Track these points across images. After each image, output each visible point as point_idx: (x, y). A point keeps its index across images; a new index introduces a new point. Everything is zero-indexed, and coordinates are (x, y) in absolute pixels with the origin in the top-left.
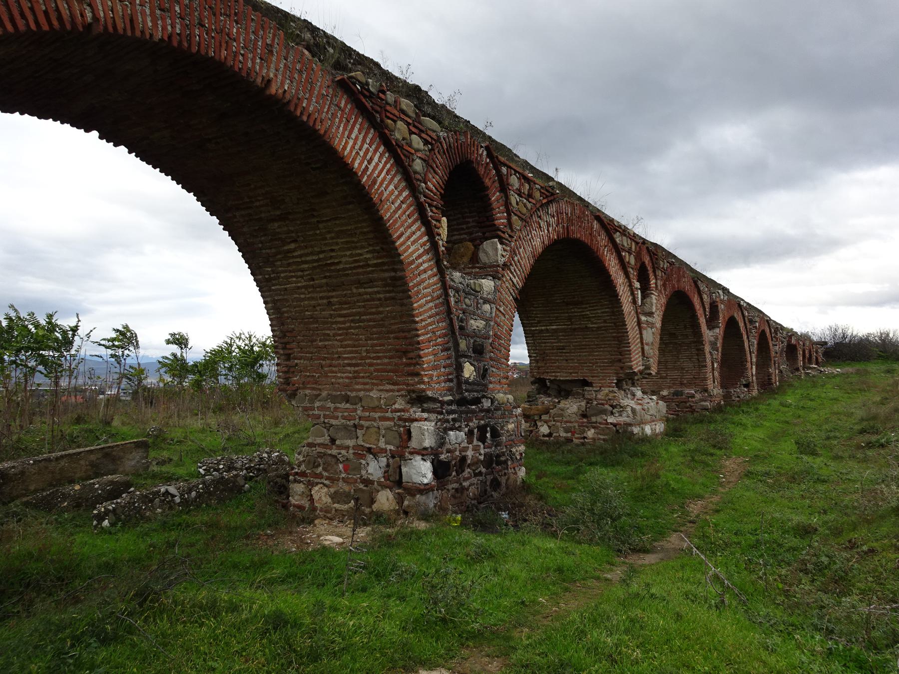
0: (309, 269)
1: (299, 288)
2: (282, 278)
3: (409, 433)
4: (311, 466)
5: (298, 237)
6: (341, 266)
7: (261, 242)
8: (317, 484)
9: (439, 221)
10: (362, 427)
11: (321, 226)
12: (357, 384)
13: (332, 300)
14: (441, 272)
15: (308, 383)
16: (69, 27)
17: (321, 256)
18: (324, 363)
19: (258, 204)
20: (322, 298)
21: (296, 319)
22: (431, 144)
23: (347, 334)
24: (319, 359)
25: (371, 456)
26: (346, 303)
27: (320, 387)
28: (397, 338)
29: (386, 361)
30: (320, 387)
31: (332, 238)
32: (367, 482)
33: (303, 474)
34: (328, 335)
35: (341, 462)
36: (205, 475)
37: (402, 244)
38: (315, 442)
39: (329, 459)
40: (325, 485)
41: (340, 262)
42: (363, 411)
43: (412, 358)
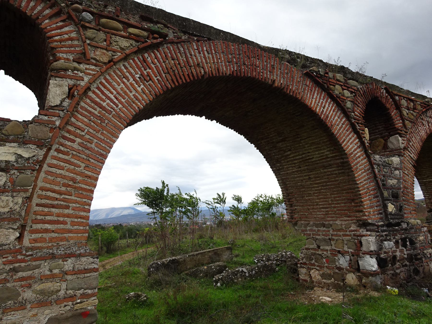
0: (298, 163)
1: (293, 172)
2: (285, 168)
3: (361, 243)
4: (309, 259)
5: (292, 148)
6: (314, 160)
7: (274, 153)
8: (313, 269)
9: (364, 130)
10: (333, 240)
11: (302, 141)
12: (328, 217)
13: (310, 176)
14: (368, 156)
15: (303, 218)
16: (196, 78)
17: (303, 156)
18: (309, 207)
19: (271, 136)
20: (305, 176)
21: (294, 187)
22: (354, 93)
23: (320, 193)
25: (341, 255)
26: (318, 177)
27: (309, 220)
28: (348, 193)
29: (343, 205)
30: (309, 220)
31: (308, 147)
32: (340, 269)
33: (305, 264)
34: (311, 194)
35: (324, 258)
36: (257, 263)
37: (345, 145)
38: (310, 248)
39: (318, 256)
40: (317, 270)
41: (313, 158)
42: (333, 231)
43: (357, 203)
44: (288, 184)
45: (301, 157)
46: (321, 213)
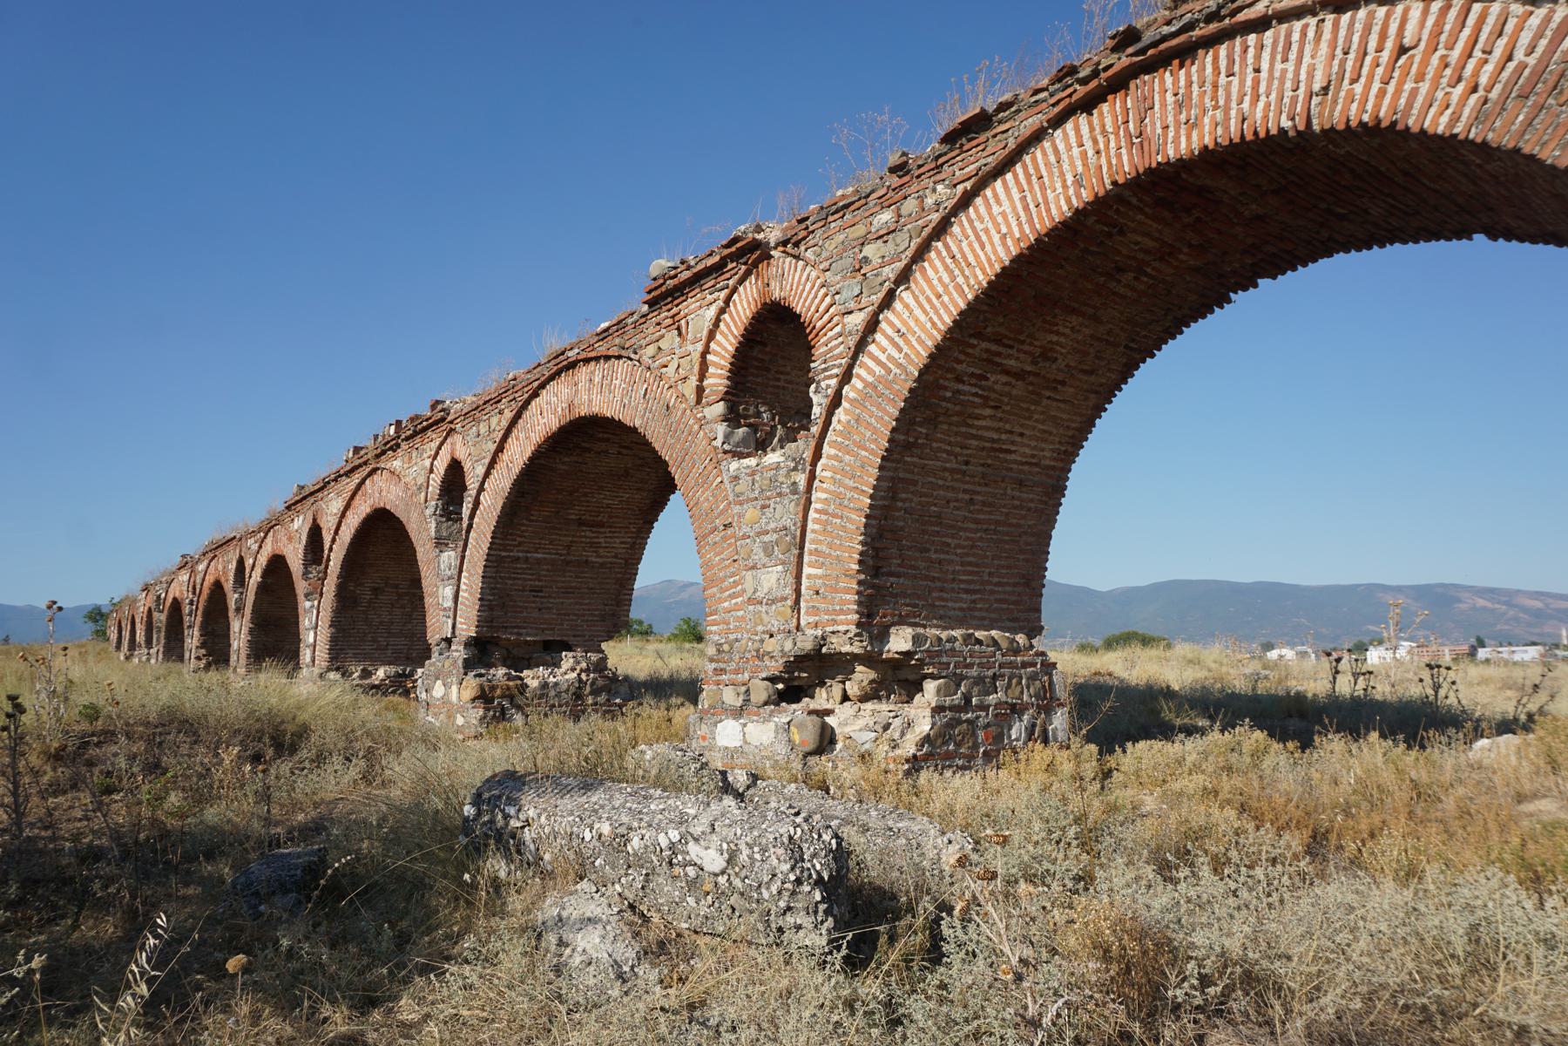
1: (945, 469)
6: (1013, 457)
13: (975, 497)
17: (1004, 437)
20: (965, 491)
24: (926, 578)
26: (990, 505)
29: (1008, 589)
34: (948, 545)
44: (904, 501)
45: (995, 436)
46: (958, 605)
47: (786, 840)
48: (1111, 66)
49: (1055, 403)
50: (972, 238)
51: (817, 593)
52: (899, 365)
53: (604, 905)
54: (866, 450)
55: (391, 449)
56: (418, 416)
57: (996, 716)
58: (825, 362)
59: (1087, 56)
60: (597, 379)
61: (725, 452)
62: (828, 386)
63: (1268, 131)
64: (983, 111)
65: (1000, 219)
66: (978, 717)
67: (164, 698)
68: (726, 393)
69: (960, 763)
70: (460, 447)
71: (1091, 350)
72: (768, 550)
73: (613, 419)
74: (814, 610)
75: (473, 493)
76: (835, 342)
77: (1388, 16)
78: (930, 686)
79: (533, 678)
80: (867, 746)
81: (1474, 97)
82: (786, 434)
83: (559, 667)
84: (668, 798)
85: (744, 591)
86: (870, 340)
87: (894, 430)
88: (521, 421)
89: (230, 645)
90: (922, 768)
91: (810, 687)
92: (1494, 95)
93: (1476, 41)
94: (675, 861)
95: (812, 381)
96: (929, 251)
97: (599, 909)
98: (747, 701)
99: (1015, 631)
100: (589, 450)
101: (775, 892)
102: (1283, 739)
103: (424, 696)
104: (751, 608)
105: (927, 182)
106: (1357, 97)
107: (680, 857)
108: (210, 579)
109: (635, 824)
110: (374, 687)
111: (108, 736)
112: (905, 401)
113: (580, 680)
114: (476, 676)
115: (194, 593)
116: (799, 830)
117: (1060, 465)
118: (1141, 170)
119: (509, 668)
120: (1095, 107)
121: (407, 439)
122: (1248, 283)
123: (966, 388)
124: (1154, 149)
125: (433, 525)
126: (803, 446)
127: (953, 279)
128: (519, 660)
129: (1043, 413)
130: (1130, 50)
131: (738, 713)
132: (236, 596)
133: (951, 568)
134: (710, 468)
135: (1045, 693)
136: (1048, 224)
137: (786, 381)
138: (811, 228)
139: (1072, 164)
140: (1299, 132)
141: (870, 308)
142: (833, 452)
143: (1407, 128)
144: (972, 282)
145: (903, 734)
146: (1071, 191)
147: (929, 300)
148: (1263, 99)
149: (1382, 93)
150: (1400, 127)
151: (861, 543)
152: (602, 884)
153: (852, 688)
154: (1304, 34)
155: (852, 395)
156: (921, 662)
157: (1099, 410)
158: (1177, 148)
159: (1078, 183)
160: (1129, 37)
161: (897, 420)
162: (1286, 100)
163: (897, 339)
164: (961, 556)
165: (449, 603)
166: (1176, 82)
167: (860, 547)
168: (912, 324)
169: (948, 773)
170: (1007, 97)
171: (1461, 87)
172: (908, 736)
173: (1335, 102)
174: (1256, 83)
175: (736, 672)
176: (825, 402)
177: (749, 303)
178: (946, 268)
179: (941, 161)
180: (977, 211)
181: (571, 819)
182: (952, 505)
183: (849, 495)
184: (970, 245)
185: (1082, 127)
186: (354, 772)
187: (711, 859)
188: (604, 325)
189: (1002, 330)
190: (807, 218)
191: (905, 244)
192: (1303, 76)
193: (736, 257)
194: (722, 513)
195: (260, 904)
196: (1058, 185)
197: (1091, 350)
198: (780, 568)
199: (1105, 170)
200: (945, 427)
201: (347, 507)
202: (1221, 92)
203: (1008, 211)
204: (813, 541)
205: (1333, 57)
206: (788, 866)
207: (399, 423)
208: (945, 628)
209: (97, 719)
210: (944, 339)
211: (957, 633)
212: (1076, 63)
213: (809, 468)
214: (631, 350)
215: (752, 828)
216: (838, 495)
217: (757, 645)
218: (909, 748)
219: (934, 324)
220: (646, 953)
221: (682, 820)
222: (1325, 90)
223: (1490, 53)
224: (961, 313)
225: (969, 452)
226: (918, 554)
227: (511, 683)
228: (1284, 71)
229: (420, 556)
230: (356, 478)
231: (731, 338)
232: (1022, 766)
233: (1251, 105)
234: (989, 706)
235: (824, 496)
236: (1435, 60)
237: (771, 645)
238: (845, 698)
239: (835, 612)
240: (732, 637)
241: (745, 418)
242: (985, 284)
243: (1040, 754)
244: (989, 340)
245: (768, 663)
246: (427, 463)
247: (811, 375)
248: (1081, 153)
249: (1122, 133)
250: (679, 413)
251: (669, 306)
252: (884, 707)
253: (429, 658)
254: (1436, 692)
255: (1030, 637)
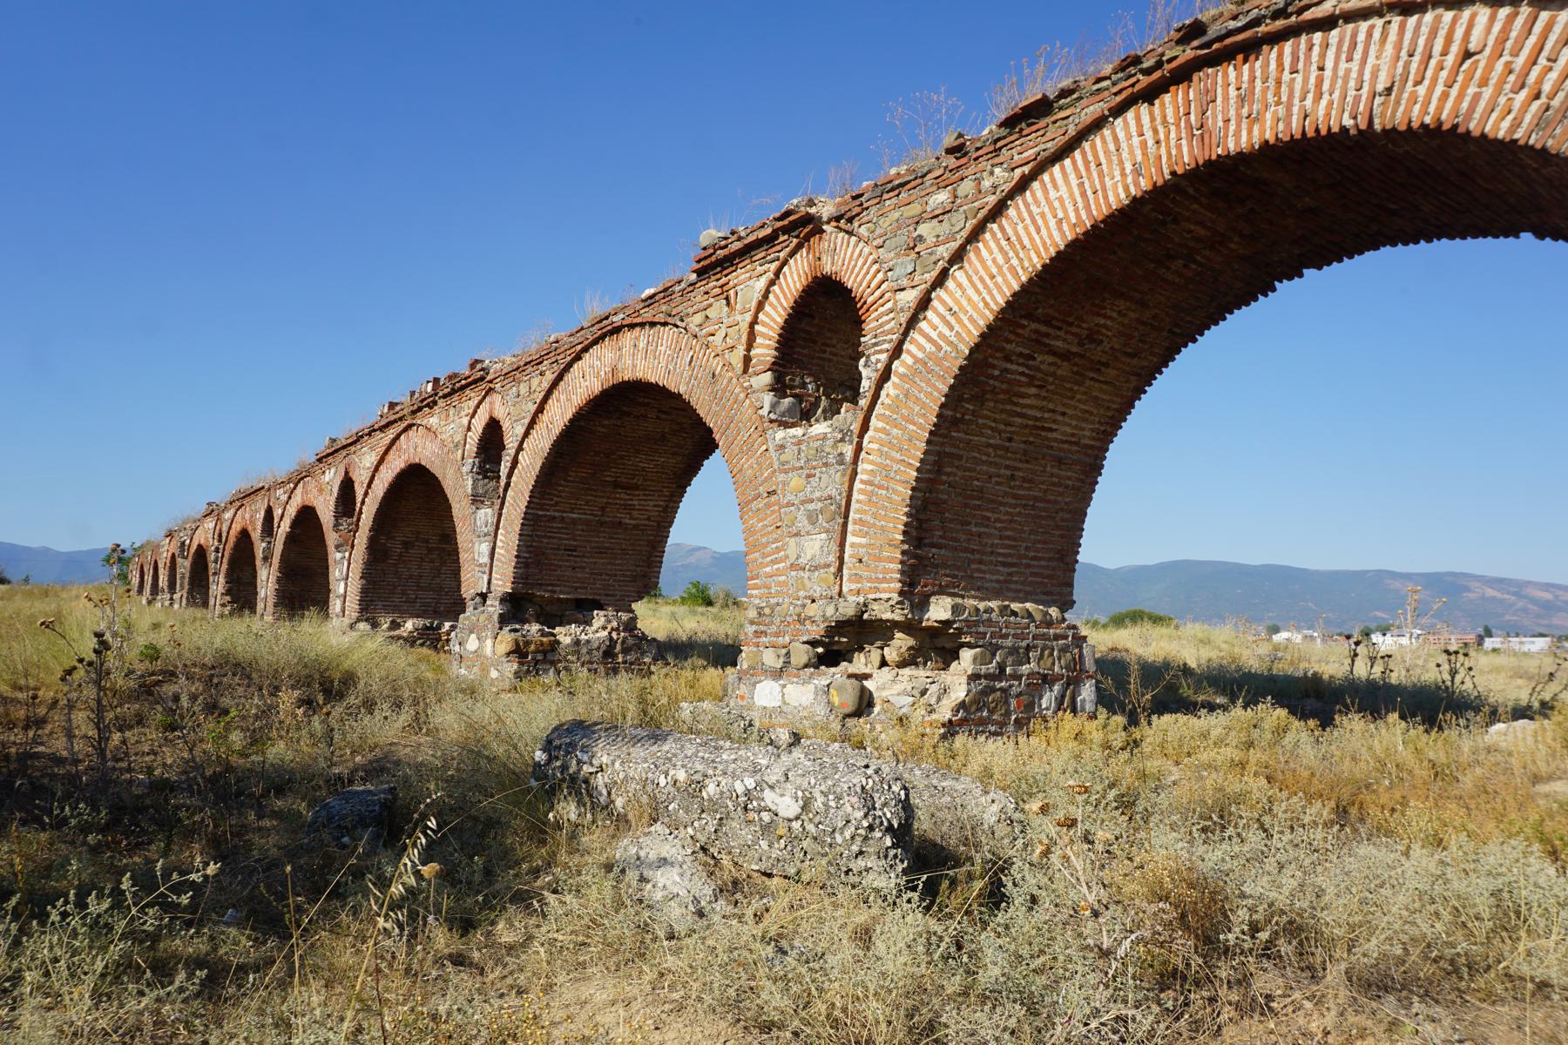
1: (989, 445)
6: (1054, 435)
13: (1016, 473)
17: (1046, 415)
20: (1007, 467)
24: (966, 550)
26: (1030, 481)
29: (1043, 563)
34: (988, 519)
44: (948, 474)
45: (1039, 415)
46: (995, 577)
47: (859, 790)
48: (1175, 58)
49: (1097, 385)
50: (1028, 221)
51: (860, 561)
52: (950, 343)
53: (679, 846)
54: (914, 424)
55: (428, 405)
56: (455, 375)
57: (1028, 685)
58: (876, 336)
59: (1150, 47)
60: (642, 345)
61: (771, 421)
62: (878, 361)
63: (1329, 129)
64: (1045, 97)
65: (1056, 204)
66: (1011, 686)
67: (218, 642)
68: (774, 363)
69: (993, 729)
70: (497, 406)
71: (1136, 334)
72: (812, 518)
73: (657, 385)
74: (857, 578)
75: (512, 452)
76: (885, 318)
77: (1454, 21)
78: (967, 655)
79: (565, 635)
80: (904, 710)
81: (1536, 104)
82: (830, 406)
83: (591, 625)
84: (739, 749)
85: (787, 557)
86: (921, 317)
87: (942, 406)
88: (562, 383)
89: (256, 593)
90: (958, 733)
91: (848, 651)
92: (1556, 102)
93: (1541, 49)
94: (750, 806)
95: (861, 355)
96: (984, 232)
97: (674, 850)
98: (787, 663)
99: (1048, 604)
100: (628, 414)
101: (848, 837)
102: (1304, 716)
103: (457, 648)
104: (793, 573)
105: (985, 164)
106: (1420, 99)
107: (755, 803)
108: (236, 528)
109: (710, 772)
110: (399, 637)
111: (171, 675)
112: (955, 377)
113: (611, 639)
114: (511, 631)
115: (220, 541)
116: (870, 781)
117: (1098, 444)
118: (1201, 162)
119: (542, 624)
120: (1157, 97)
121: (444, 396)
122: (1294, 272)
123: (1014, 367)
124: (1214, 141)
125: (470, 482)
126: (848, 416)
127: (1008, 260)
128: (552, 617)
129: (1085, 393)
130: (1195, 43)
131: (778, 674)
132: (264, 545)
133: (990, 542)
134: (755, 436)
135: (1075, 664)
136: (1105, 211)
137: (832, 353)
138: (865, 205)
139: (1132, 152)
140: (1359, 131)
141: (923, 286)
142: (880, 424)
143: (1468, 132)
144: (1026, 264)
145: (939, 700)
146: (1130, 179)
147: (982, 280)
148: (1326, 97)
149: (1445, 96)
150: (1461, 130)
151: (907, 514)
152: (674, 826)
153: (891, 654)
154: (1369, 35)
155: (902, 370)
156: (960, 632)
157: (1139, 392)
158: (1237, 142)
159: (1137, 172)
160: (1194, 30)
161: (946, 396)
162: (1350, 99)
163: (949, 318)
164: (1000, 529)
165: (485, 559)
166: (1239, 76)
167: (905, 518)
168: (964, 303)
169: (982, 739)
170: (1066, 83)
171: (1523, 94)
172: (944, 702)
173: (1398, 103)
174: (1320, 81)
175: (777, 635)
176: (875, 376)
177: (800, 276)
178: (1001, 249)
179: (999, 144)
180: (1033, 195)
181: (646, 765)
182: (994, 480)
183: (895, 467)
184: (1026, 228)
185: (1143, 117)
186: (405, 717)
187: (787, 806)
188: (650, 291)
189: (1051, 311)
190: (862, 195)
191: (961, 225)
192: (1367, 76)
193: (786, 230)
194: (766, 480)
195: (343, 836)
196: (1117, 173)
197: (1136, 334)
198: (824, 536)
199: (1164, 160)
200: (992, 404)
201: (381, 461)
202: (1284, 88)
203: (1066, 196)
204: (858, 511)
205: (1398, 58)
206: (862, 814)
207: (436, 380)
208: (982, 599)
209: (156, 659)
210: (997, 319)
211: (994, 604)
212: (1140, 53)
213: (856, 440)
214: (677, 318)
215: (825, 778)
216: (885, 467)
217: (798, 610)
218: (945, 713)
219: (986, 304)
220: (721, 891)
221: (756, 770)
222: (1389, 90)
223: (1555, 61)
224: (1015, 295)
225: (1013, 429)
226: (959, 527)
227: (545, 639)
228: (1348, 71)
229: (455, 512)
230: (391, 434)
231: (780, 309)
232: (1052, 733)
233: (1314, 102)
234: (1022, 676)
235: (870, 467)
236: (1499, 66)
237: (812, 610)
238: (884, 663)
239: (878, 580)
240: (773, 601)
241: (792, 388)
242: (1039, 267)
243: (1069, 723)
244: (1038, 321)
245: (809, 627)
246: (465, 421)
247: (860, 349)
248: (1141, 142)
249: (1183, 124)
250: (725, 382)
251: (718, 276)
252: (921, 673)
253: (464, 612)
254: (1453, 678)
255: (1063, 611)
